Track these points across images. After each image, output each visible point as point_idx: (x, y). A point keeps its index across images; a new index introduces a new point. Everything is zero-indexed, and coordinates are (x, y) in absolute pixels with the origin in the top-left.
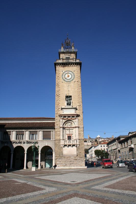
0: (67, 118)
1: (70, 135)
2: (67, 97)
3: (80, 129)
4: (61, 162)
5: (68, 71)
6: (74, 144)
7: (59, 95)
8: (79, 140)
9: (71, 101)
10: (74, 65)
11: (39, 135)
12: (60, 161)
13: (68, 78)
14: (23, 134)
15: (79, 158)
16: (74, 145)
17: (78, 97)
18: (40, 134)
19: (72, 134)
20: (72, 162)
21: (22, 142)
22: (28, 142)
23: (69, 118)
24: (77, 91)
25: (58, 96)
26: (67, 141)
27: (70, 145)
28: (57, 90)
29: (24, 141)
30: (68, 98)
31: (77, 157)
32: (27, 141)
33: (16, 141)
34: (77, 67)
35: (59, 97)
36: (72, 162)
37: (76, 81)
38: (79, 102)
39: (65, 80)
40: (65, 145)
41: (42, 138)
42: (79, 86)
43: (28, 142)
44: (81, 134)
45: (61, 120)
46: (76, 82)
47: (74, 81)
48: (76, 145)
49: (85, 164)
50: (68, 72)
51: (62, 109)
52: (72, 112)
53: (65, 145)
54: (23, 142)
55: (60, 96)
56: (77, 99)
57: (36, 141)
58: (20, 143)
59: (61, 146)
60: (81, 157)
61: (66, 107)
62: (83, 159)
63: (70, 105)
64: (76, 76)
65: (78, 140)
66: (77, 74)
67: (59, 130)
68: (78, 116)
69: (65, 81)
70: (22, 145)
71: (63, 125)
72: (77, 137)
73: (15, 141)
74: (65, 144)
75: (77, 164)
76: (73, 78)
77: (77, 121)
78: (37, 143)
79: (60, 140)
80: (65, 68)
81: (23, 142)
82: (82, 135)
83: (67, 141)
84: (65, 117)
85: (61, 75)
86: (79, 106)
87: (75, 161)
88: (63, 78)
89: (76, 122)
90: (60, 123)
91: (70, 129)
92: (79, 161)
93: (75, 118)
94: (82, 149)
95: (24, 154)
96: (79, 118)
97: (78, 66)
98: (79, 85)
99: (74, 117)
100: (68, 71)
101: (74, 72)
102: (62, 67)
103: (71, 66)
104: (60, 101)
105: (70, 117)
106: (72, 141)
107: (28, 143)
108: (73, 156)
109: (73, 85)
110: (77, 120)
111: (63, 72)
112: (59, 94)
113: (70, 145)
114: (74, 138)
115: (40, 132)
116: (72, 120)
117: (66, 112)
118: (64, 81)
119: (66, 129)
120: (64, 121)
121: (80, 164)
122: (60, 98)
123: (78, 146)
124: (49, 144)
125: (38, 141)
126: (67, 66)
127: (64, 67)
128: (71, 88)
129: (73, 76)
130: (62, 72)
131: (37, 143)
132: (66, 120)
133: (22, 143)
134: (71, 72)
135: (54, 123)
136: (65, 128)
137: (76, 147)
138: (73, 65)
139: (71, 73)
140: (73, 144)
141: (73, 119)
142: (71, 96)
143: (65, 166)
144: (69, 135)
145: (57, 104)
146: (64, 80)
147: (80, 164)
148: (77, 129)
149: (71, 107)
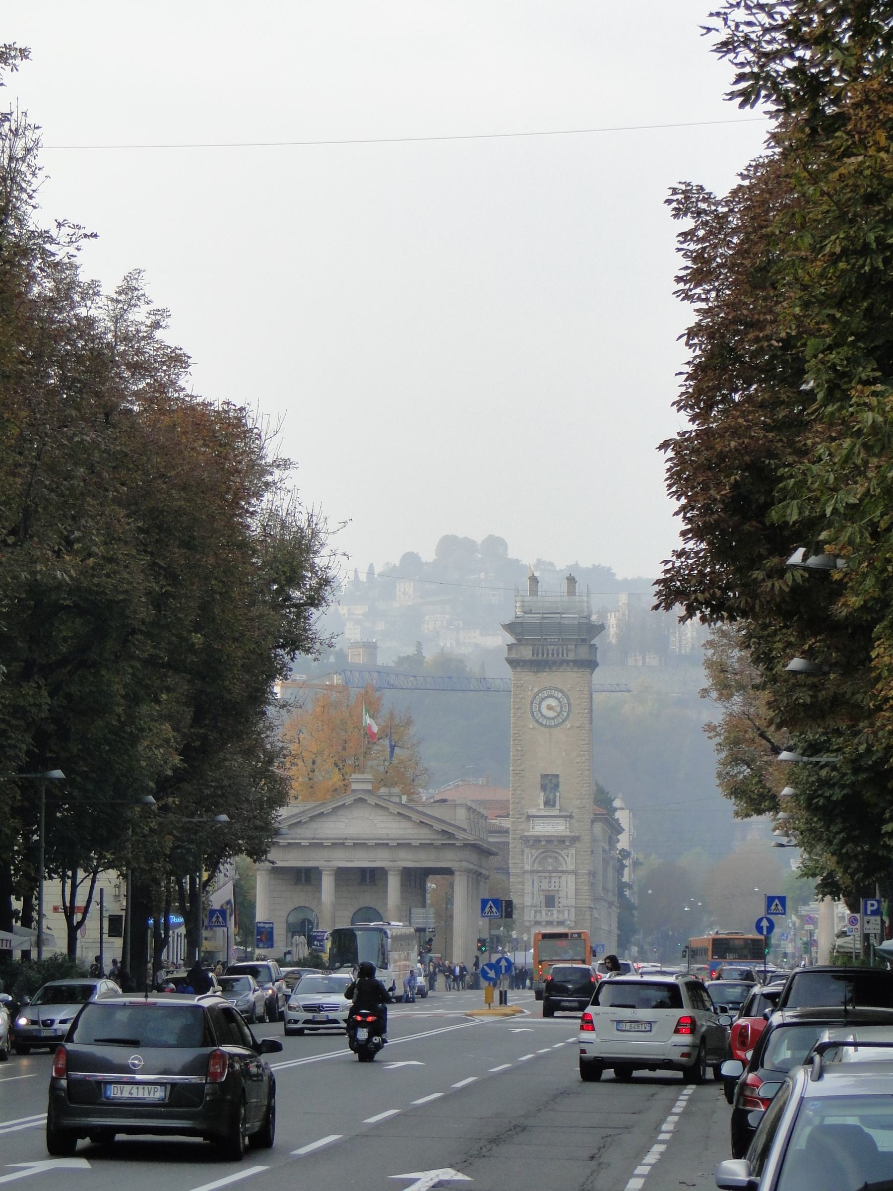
1: (551, 894)
5: (550, 688)
6: (561, 919)
8: (576, 907)
9: (558, 794)
26: (544, 913)
30: (550, 784)
42: (583, 742)
45: (527, 850)
47: (568, 724)
50: (549, 692)
51: (529, 817)
52: (559, 828)
59: (527, 924)
61: (542, 813)
63: (554, 805)
65: (573, 910)
67: (520, 880)
68: (575, 839)
69: (541, 724)
72: (572, 902)
74: (538, 918)
76: (565, 714)
83: (544, 913)
89: (569, 859)
91: (553, 874)
96: (578, 845)
100: (550, 688)
106: (555, 912)
111: (536, 690)
112: (520, 768)
114: (564, 902)
117: (541, 829)
127: (538, 672)
134: (561, 691)
139: (560, 695)
141: (562, 850)
144: (547, 893)
146: (537, 721)
149: (556, 813)
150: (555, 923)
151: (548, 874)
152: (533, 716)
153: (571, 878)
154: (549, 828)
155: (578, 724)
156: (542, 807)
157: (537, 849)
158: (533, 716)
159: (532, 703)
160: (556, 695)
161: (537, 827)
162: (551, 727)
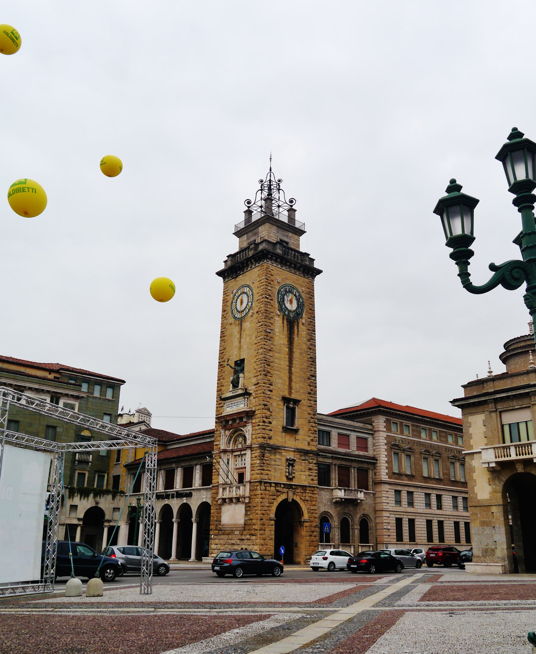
0: (231, 425)
15: (248, 537)
16: (238, 500)
17: (255, 360)
21: (169, 494)
24: (256, 342)
25: (221, 365)
29: (173, 493)
32: (177, 492)
38: (257, 374)
39: (236, 316)
43: (179, 495)
47: (251, 311)
53: (224, 500)
56: (254, 364)
66: (258, 291)
71: (229, 443)
76: (250, 304)
77: (249, 430)
78: (189, 495)
79: (218, 486)
82: (258, 468)
91: (243, 452)
93: (246, 422)
98: (259, 322)
102: (233, 280)
103: (249, 269)
110: (249, 427)
111: (235, 292)
113: (231, 499)
129: (250, 300)
130: (231, 295)
131: (189, 495)
134: (248, 286)
138: (252, 264)
139: (248, 289)
142: (243, 361)
149: (240, 392)
150: (234, 500)
151: (238, 453)
152: (232, 313)
155: (256, 309)
156: (231, 389)
157: (229, 430)
158: (232, 313)
159: (232, 303)
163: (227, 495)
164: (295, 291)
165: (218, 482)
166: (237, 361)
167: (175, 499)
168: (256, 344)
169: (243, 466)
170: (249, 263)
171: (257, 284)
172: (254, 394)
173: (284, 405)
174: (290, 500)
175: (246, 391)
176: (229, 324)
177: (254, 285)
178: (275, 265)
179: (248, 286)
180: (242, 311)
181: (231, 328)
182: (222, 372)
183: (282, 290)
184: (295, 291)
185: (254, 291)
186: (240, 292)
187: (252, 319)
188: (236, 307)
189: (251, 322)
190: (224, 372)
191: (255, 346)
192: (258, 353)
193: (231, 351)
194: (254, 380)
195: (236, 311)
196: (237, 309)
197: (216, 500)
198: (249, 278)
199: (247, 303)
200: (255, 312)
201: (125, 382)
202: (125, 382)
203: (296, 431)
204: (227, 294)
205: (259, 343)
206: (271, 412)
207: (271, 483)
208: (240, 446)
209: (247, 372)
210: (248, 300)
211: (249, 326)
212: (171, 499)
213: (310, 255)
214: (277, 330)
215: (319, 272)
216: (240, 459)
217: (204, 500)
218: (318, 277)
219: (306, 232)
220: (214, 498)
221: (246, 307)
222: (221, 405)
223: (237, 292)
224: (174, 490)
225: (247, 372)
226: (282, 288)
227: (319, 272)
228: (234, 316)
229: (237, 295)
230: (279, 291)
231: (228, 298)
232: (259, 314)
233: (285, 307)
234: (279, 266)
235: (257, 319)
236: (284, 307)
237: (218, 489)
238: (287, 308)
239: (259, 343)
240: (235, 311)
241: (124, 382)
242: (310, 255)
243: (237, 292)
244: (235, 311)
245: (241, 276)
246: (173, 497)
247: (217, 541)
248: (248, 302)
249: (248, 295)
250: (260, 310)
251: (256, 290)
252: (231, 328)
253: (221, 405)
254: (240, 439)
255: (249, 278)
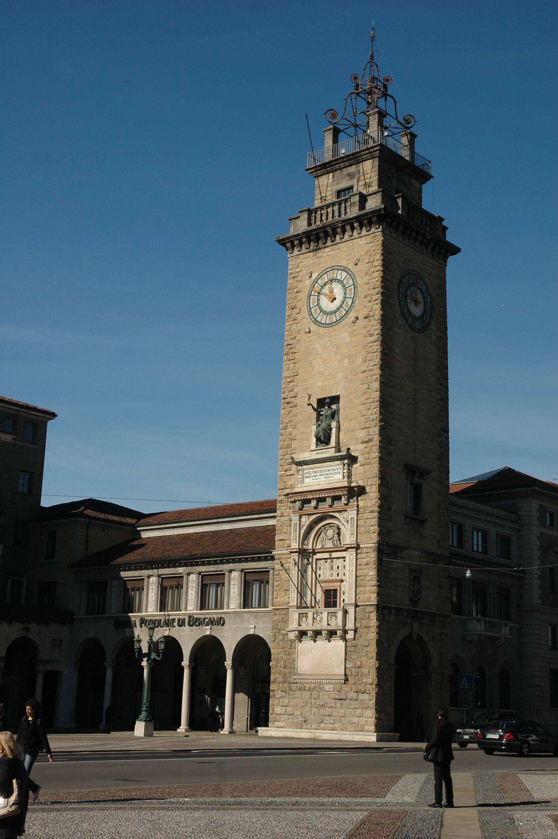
2: (321, 402)
3: (364, 555)
4: (288, 709)
5: (333, 269)
7: (295, 401)
8: (356, 606)
10: (355, 233)
11: (232, 587)
12: (286, 701)
13: (337, 303)
14: (179, 587)
16: (332, 634)
17: (363, 399)
18: (232, 583)
19: (342, 581)
20: (327, 711)
22: (194, 622)
23: (324, 507)
24: (364, 368)
25: (288, 403)
27: (317, 633)
28: (286, 377)
29: (182, 617)
31: (346, 688)
33: (157, 618)
34: (368, 239)
35: (295, 410)
36: (327, 711)
37: (361, 317)
38: (367, 425)
39: (319, 319)
40: (302, 634)
41: (238, 602)
43: (194, 622)
44: (368, 578)
46: (361, 322)
47: (352, 315)
48: (339, 633)
49: (372, 721)
53: (302, 634)
54: (176, 621)
55: (296, 406)
56: (361, 408)
57: (219, 616)
58: (169, 623)
60: (361, 688)
62: (366, 696)
64: (362, 292)
65: (351, 610)
66: (366, 279)
70: (175, 632)
73: (154, 618)
75: (343, 719)
76: (350, 301)
77: (353, 518)
78: (220, 622)
80: (320, 253)
81: (179, 620)
84: (308, 501)
85: (303, 295)
86: (363, 443)
87: (339, 703)
88: (313, 310)
90: (290, 533)
91: (334, 555)
92: (354, 704)
94: (365, 649)
95: (182, 669)
97: (373, 230)
98: (371, 335)
99: (339, 498)
100: (333, 269)
101: (355, 270)
102: (311, 254)
103: (346, 237)
104: (295, 427)
105: (323, 500)
107: (192, 626)
108: (330, 679)
109: (348, 339)
111: (314, 276)
112: (292, 394)
113: (317, 633)
115: (233, 574)
116: (336, 514)
118: (313, 327)
119: (318, 556)
120: (306, 521)
121: (356, 720)
122: (295, 415)
123: (350, 635)
124: (261, 626)
125: (225, 613)
126: (329, 243)
128: (339, 357)
129: (351, 293)
130: (307, 282)
132: (314, 517)
133: (175, 624)
134: (345, 269)
135: (272, 530)
136: (314, 553)
137: (344, 638)
139: (344, 274)
140: (329, 628)
142: (335, 399)
143: (301, 728)
145: (286, 443)
146: (316, 322)
147: (356, 720)
148: (350, 555)
149: (331, 453)
151: (327, 555)
152: (311, 314)
153: (350, 555)
154: (322, 478)
155: (365, 312)
156: (313, 447)
158: (311, 314)
160: (339, 277)
161: (306, 480)
162: (331, 324)
163: (308, 625)
164: (421, 282)
165: (289, 603)
166: (325, 399)
167: (187, 627)
168: (363, 372)
169: (334, 577)
170: (348, 228)
171: (363, 267)
172: (360, 459)
173: (407, 479)
174: (415, 636)
175: (348, 452)
176: (302, 332)
177: (357, 269)
178: (394, 235)
179: (345, 269)
180: (331, 313)
181: (307, 340)
182: (290, 415)
183: (404, 280)
184: (421, 282)
185: (358, 279)
186: (326, 278)
187: (355, 328)
188: (318, 304)
189: (352, 334)
190: (295, 415)
191: (361, 375)
192: (368, 388)
193: (309, 381)
194: (362, 434)
195: (319, 311)
196: (320, 307)
197: (285, 632)
198: (347, 256)
199: (342, 299)
200: (361, 317)
201: (56, 416)
202: (56, 416)
203: (423, 522)
204: (299, 279)
205: (371, 370)
206: (390, 490)
207: (390, 608)
208: (329, 545)
209: (345, 419)
210: (345, 293)
211: (348, 339)
212: (177, 627)
213: (443, 220)
214: (397, 350)
215: (455, 250)
216: (327, 565)
217: (252, 632)
218: (451, 260)
219: (433, 177)
220: (277, 629)
221: (341, 306)
222: (289, 473)
223: (320, 277)
224: (183, 612)
225: (345, 419)
226: (404, 277)
227: (455, 250)
228: (316, 319)
229: (319, 281)
230: (400, 282)
231: (300, 285)
232: (370, 321)
233: (408, 310)
234: (400, 238)
235: (366, 330)
236: (406, 310)
237: (287, 615)
238: (410, 313)
239: (371, 370)
240: (316, 311)
241: (53, 415)
242: (443, 220)
243: (320, 277)
244: (316, 311)
245: (327, 250)
246: (181, 623)
247: (286, 701)
248: (345, 298)
249: (344, 286)
250: (371, 314)
251: (361, 277)
252: (307, 340)
253: (289, 473)
254: (330, 532)
255: (347, 256)
